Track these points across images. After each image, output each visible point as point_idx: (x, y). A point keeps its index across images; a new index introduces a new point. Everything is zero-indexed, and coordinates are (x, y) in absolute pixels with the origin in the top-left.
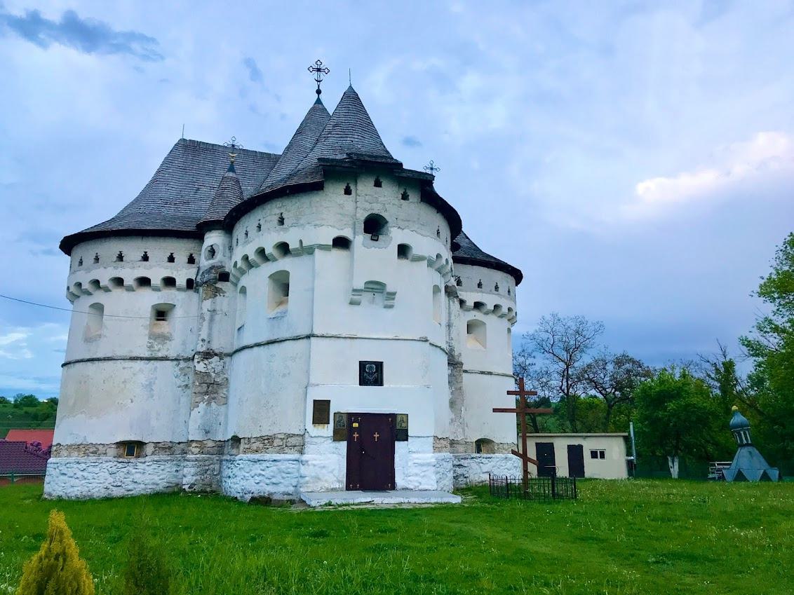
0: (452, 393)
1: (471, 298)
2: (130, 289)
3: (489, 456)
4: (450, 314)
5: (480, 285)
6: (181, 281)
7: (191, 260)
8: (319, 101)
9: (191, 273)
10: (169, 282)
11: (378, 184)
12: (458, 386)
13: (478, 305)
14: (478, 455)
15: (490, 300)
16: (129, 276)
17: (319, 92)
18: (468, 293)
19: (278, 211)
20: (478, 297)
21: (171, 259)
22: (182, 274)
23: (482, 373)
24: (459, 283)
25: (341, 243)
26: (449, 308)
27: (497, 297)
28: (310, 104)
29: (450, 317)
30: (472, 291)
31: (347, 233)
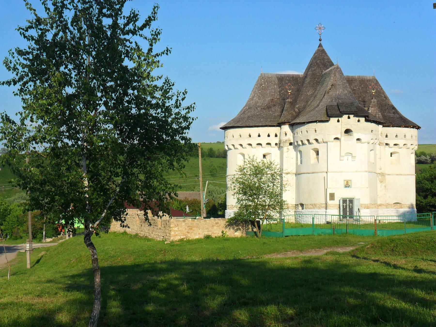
2: (255, 148)
6: (273, 144)
7: (276, 136)
8: (320, 46)
9: (277, 140)
10: (269, 144)
11: (349, 118)
15: (401, 142)
16: (254, 142)
17: (320, 40)
19: (314, 128)
21: (269, 136)
22: (274, 140)
25: (337, 139)
28: (316, 48)
31: (339, 136)
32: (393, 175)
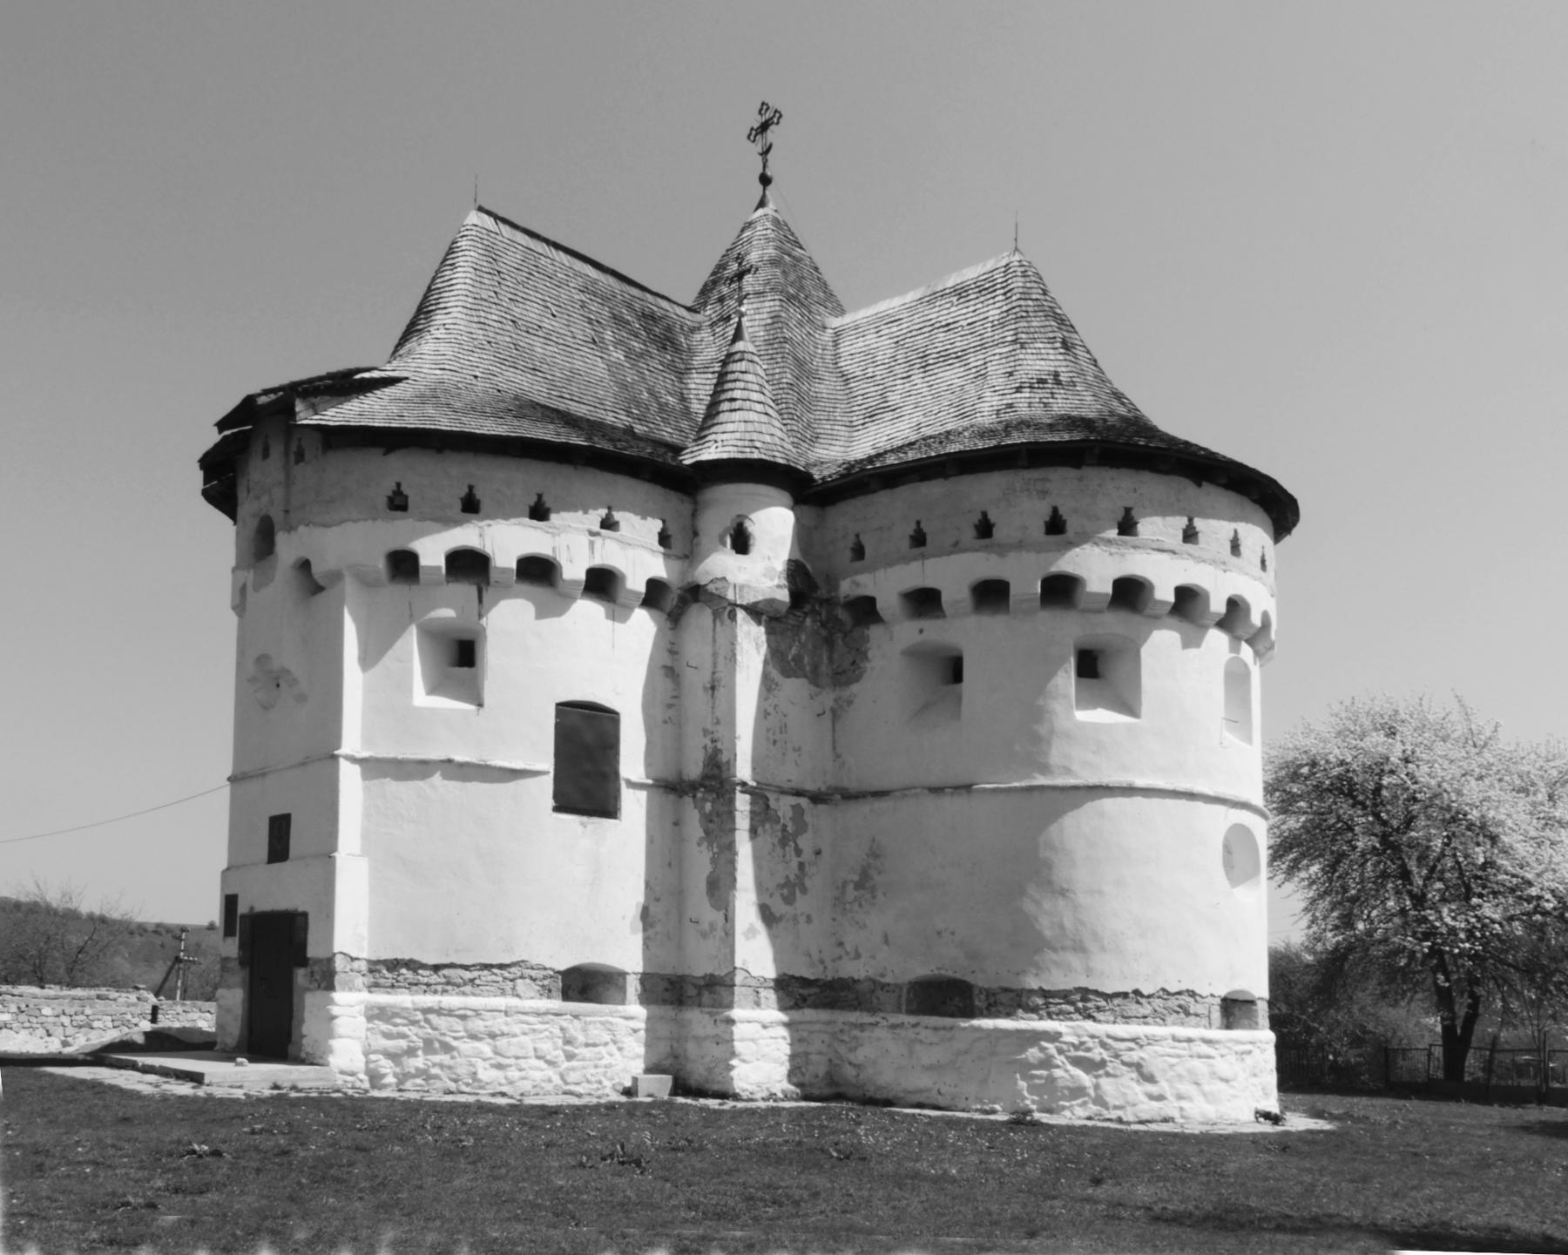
0: (714, 861)
1: (886, 585)
3: (948, 1021)
4: (715, 655)
5: (919, 539)
12: (725, 840)
13: (925, 601)
14: (912, 1019)
15: (951, 575)
18: (881, 574)
20: (914, 575)
23: (936, 790)
24: (859, 552)
26: (714, 640)
27: (979, 557)
29: (715, 664)
30: (890, 564)
32: (906, 791)
